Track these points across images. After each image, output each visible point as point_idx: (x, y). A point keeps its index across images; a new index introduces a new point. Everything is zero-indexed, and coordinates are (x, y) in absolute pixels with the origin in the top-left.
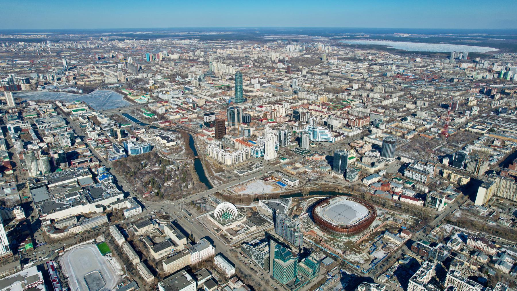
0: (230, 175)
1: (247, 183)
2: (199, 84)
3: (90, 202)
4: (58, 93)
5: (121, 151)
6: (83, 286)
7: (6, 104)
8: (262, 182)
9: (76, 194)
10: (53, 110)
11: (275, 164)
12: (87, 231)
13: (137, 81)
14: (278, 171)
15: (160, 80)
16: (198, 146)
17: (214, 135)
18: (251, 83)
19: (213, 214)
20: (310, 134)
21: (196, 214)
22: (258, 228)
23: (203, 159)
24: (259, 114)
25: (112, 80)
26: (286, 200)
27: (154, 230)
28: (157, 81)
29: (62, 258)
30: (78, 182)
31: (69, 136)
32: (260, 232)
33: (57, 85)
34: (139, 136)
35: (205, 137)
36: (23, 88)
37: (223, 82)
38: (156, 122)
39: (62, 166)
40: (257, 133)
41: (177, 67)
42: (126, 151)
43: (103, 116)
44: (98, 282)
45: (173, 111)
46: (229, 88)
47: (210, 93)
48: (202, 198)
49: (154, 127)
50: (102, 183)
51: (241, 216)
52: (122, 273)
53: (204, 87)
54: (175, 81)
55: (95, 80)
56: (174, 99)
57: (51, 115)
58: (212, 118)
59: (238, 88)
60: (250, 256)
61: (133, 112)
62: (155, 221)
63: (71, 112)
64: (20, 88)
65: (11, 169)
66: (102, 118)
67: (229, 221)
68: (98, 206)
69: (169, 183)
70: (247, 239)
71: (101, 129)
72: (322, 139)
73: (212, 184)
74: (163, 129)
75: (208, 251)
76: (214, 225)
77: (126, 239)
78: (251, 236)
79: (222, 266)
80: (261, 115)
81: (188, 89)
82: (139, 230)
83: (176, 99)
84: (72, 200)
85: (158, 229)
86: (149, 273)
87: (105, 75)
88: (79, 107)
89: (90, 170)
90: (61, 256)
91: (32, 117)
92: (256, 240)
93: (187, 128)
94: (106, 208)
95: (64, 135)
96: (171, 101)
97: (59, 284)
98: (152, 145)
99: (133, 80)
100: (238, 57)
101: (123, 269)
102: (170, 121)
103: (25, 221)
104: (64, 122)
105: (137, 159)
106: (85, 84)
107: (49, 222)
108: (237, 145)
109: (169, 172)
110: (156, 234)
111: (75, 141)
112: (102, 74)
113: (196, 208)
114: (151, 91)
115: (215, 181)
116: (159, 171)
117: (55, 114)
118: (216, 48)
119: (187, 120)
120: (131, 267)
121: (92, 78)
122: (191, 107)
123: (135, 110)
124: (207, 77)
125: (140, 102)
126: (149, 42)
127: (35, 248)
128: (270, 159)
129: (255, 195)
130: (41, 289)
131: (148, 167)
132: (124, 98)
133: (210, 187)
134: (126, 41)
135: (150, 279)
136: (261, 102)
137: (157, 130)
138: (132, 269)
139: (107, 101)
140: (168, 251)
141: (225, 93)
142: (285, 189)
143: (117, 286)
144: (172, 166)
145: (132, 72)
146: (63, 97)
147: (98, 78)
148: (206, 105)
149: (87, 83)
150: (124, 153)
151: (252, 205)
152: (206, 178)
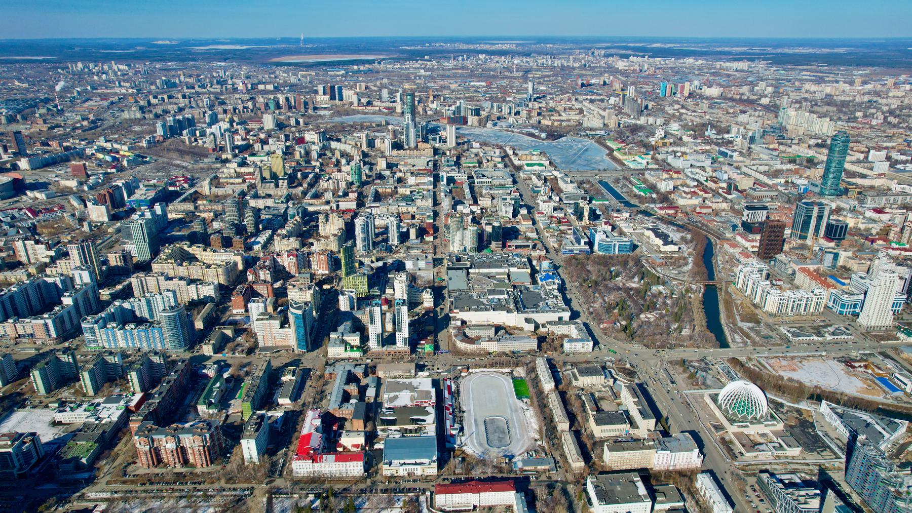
0: (771, 333)
1: (804, 358)
2: (750, 148)
3: (518, 310)
4: (512, 134)
5: (582, 241)
6: (481, 433)
7: (446, 142)
8: (840, 367)
9: (501, 293)
10: (500, 160)
11: (882, 338)
12: (504, 353)
13: (635, 129)
14: (887, 356)
15: (676, 133)
16: (720, 262)
17: (756, 249)
18: (866, 158)
19: (717, 395)
21: (684, 385)
22: (805, 456)
23: (724, 288)
24: (871, 226)
25: (595, 123)
26: (891, 422)
27: (605, 387)
28: (670, 134)
29: (463, 381)
30: (509, 276)
31: (513, 202)
32: (807, 464)
33: (513, 122)
34: (618, 223)
35: (737, 250)
36: (469, 123)
37: (802, 149)
38: (652, 206)
39: (493, 245)
40: (853, 265)
41: (712, 111)
42: (591, 244)
43: (569, 180)
44: (501, 436)
45: (687, 190)
46: (811, 163)
47: (767, 168)
48: (702, 360)
49: (646, 213)
50: (543, 286)
51: (773, 417)
52: (537, 437)
53: (758, 154)
54: (702, 136)
55: (569, 120)
56: (693, 170)
57: (495, 166)
58: (761, 216)
59: (834, 165)
60: (773, 502)
61: (617, 181)
62: (610, 372)
63: (523, 166)
64: (465, 122)
65: (432, 235)
66: (566, 182)
67: (744, 419)
68: (528, 321)
69: (649, 316)
70: (774, 466)
71: (561, 200)
73: (730, 340)
74: (661, 219)
75: (690, 459)
76: (713, 416)
77: (556, 386)
78: (783, 464)
79: (708, 495)
80: (875, 229)
81: (724, 155)
82: (581, 379)
83: (698, 170)
84: (495, 301)
85: (611, 388)
86: (578, 454)
87: (585, 113)
88: (535, 159)
89: (530, 261)
90: (464, 377)
91: (471, 165)
92: (793, 476)
93: (707, 226)
94: (539, 327)
95: (506, 199)
96: (688, 171)
97: (451, 416)
98: (636, 243)
99: (629, 126)
100: (850, 101)
101: (540, 432)
102: (677, 207)
103: (432, 312)
104: (511, 180)
105: (605, 262)
106: (552, 124)
107: (459, 323)
108: (800, 278)
109: (654, 296)
110: (605, 395)
111: (519, 212)
112: (581, 111)
113: (687, 375)
114: (655, 148)
115: (736, 336)
116: (637, 291)
117: (500, 166)
118: (803, 80)
119: (710, 210)
120: (553, 433)
121: (564, 116)
122: (723, 188)
123: (621, 178)
124: (767, 137)
125: (632, 166)
126: (671, 62)
127: (435, 354)
128: (873, 324)
129: (816, 387)
130: (430, 413)
131: (620, 278)
132: (608, 155)
133: (724, 344)
134: (631, 58)
135: (578, 464)
136: (882, 202)
137: (651, 219)
138: (553, 436)
139: (580, 157)
140: (619, 430)
141: (800, 171)
142: (896, 398)
143: (526, 454)
144: (661, 288)
145: (630, 113)
146: (517, 141)
147: (574, 117)
148: (754, 190)
149: (556, 124)
150: (587, 247)
151: (804, 406)
152: (720, 325)
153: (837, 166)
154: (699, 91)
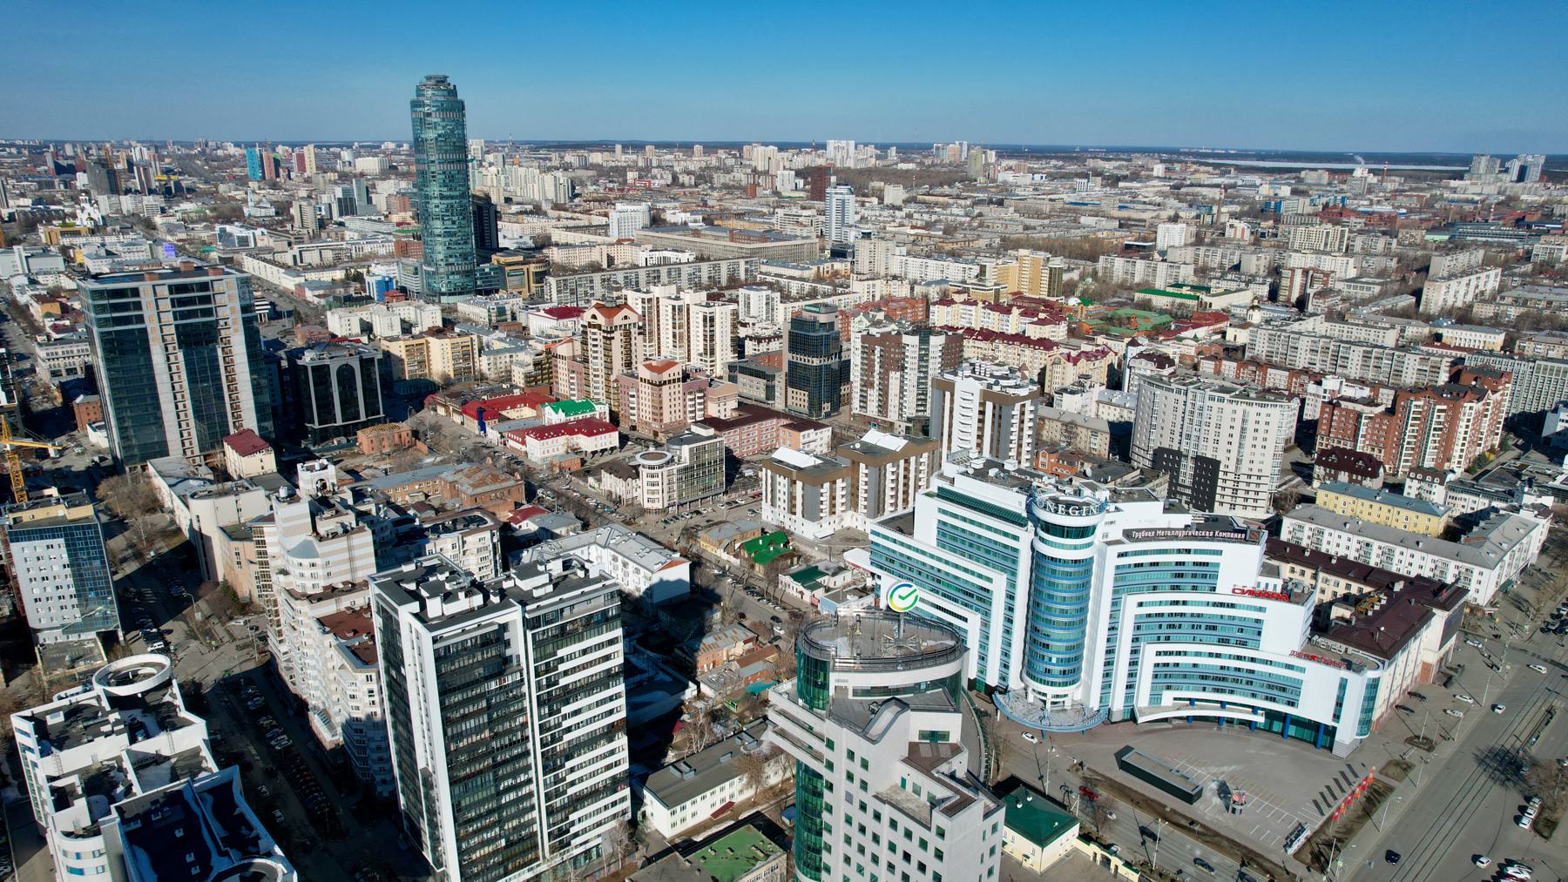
20: (979, 598)
72: (1165, 676)
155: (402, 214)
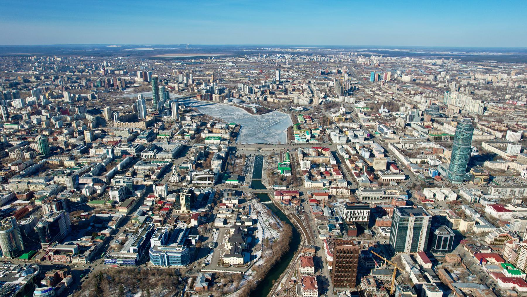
18: (504, 136)
41: (399, 92)
100: (505, 86)
118: (476, 71)
126: (394, 59)
134: (371, 57)
153: (462, 153)
154: (399, 78)
155: (429, 122)
